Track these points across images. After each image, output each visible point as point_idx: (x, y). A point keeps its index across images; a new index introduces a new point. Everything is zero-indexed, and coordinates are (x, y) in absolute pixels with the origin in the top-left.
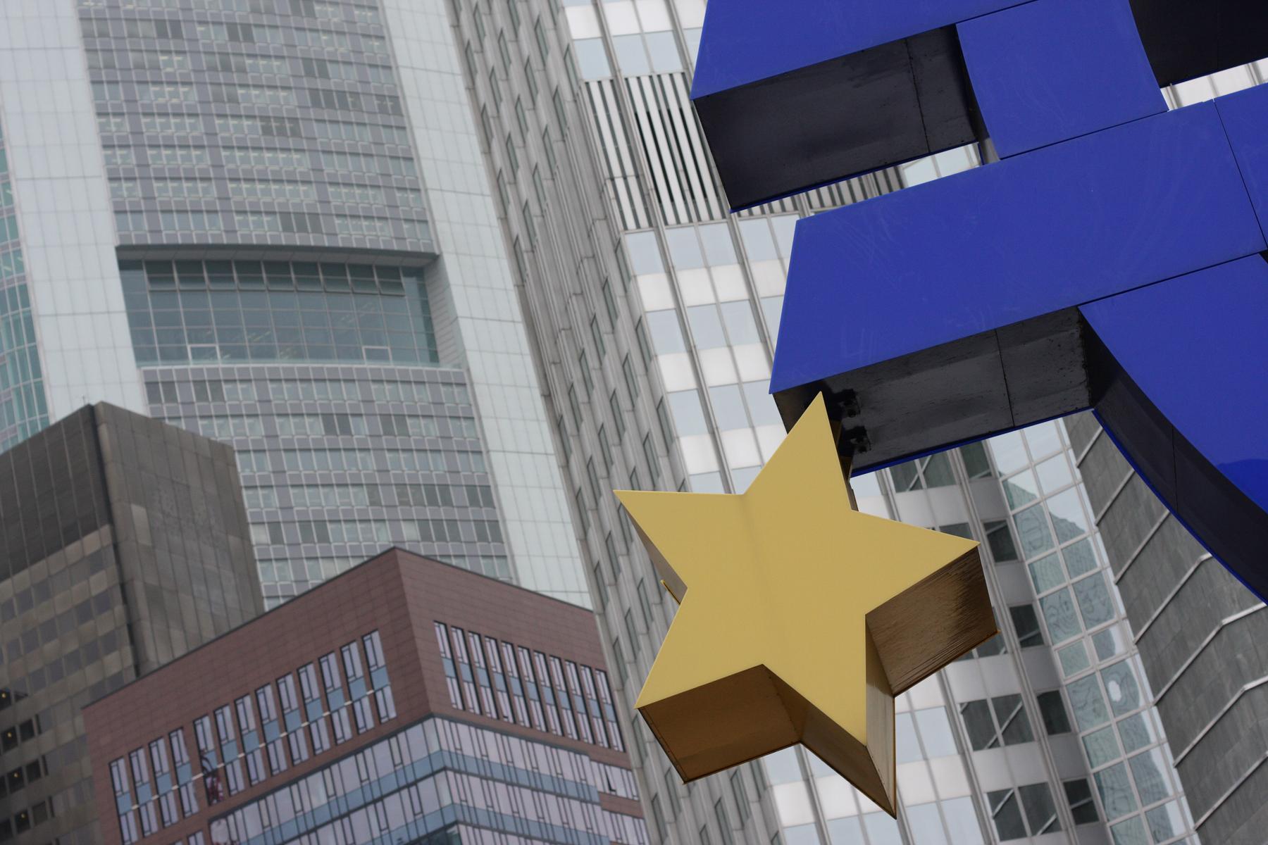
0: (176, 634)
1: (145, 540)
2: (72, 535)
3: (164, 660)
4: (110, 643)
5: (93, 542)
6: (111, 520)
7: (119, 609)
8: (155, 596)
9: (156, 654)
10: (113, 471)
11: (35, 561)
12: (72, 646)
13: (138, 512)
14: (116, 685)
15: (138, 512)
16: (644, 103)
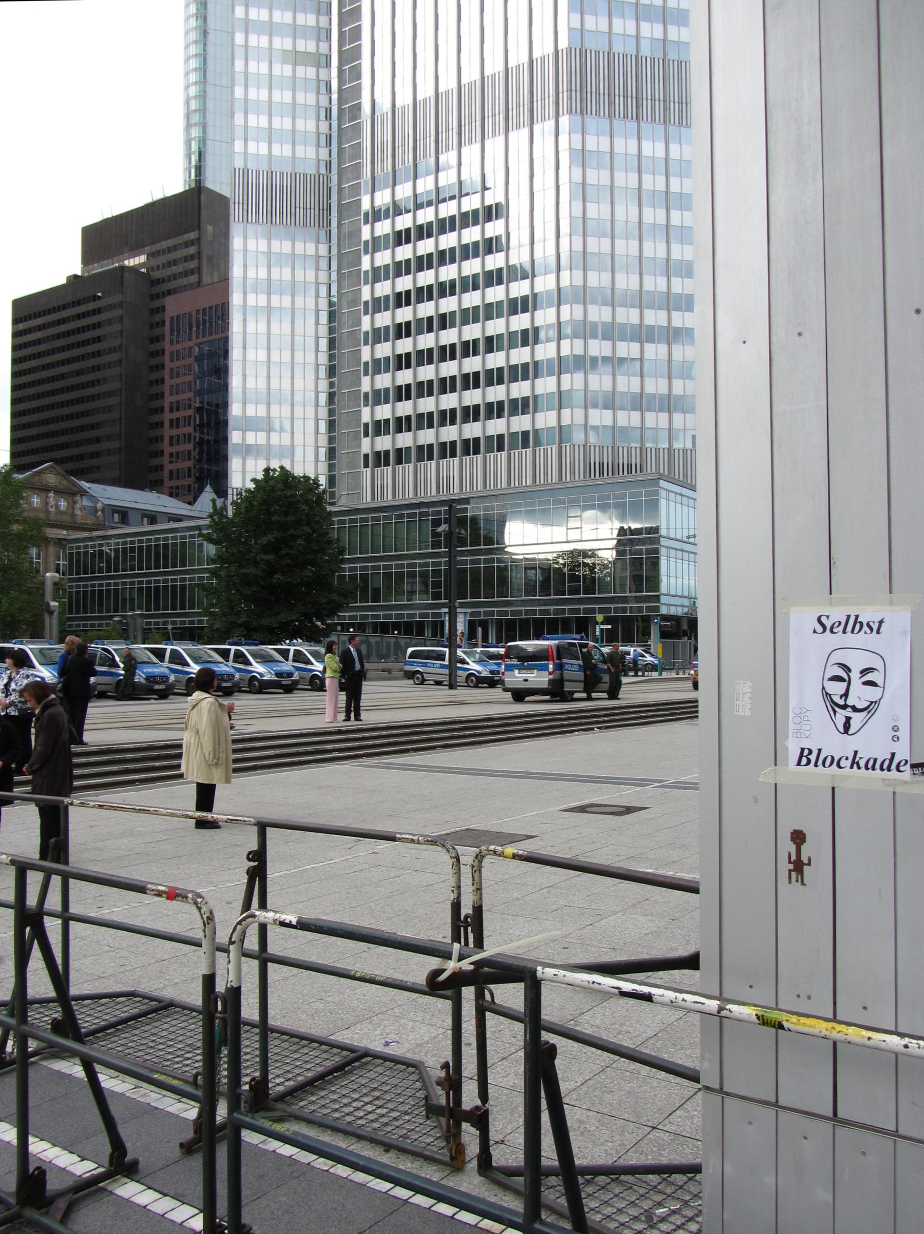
0: (216, 273)
1: (210, 238)
2: (187, 231)
3: (209, 281)
4: (192, 272)
5: (193, 235)
6: (199, 229)
7: (196, 261)
8: (210, 259)
9: (206, 279)
10: (204, 212)
11: (175, 236)
12: (181, 270)
13: (210, 228)
14: (186, 288)
15: (210, 228)
16: (253, 179)
